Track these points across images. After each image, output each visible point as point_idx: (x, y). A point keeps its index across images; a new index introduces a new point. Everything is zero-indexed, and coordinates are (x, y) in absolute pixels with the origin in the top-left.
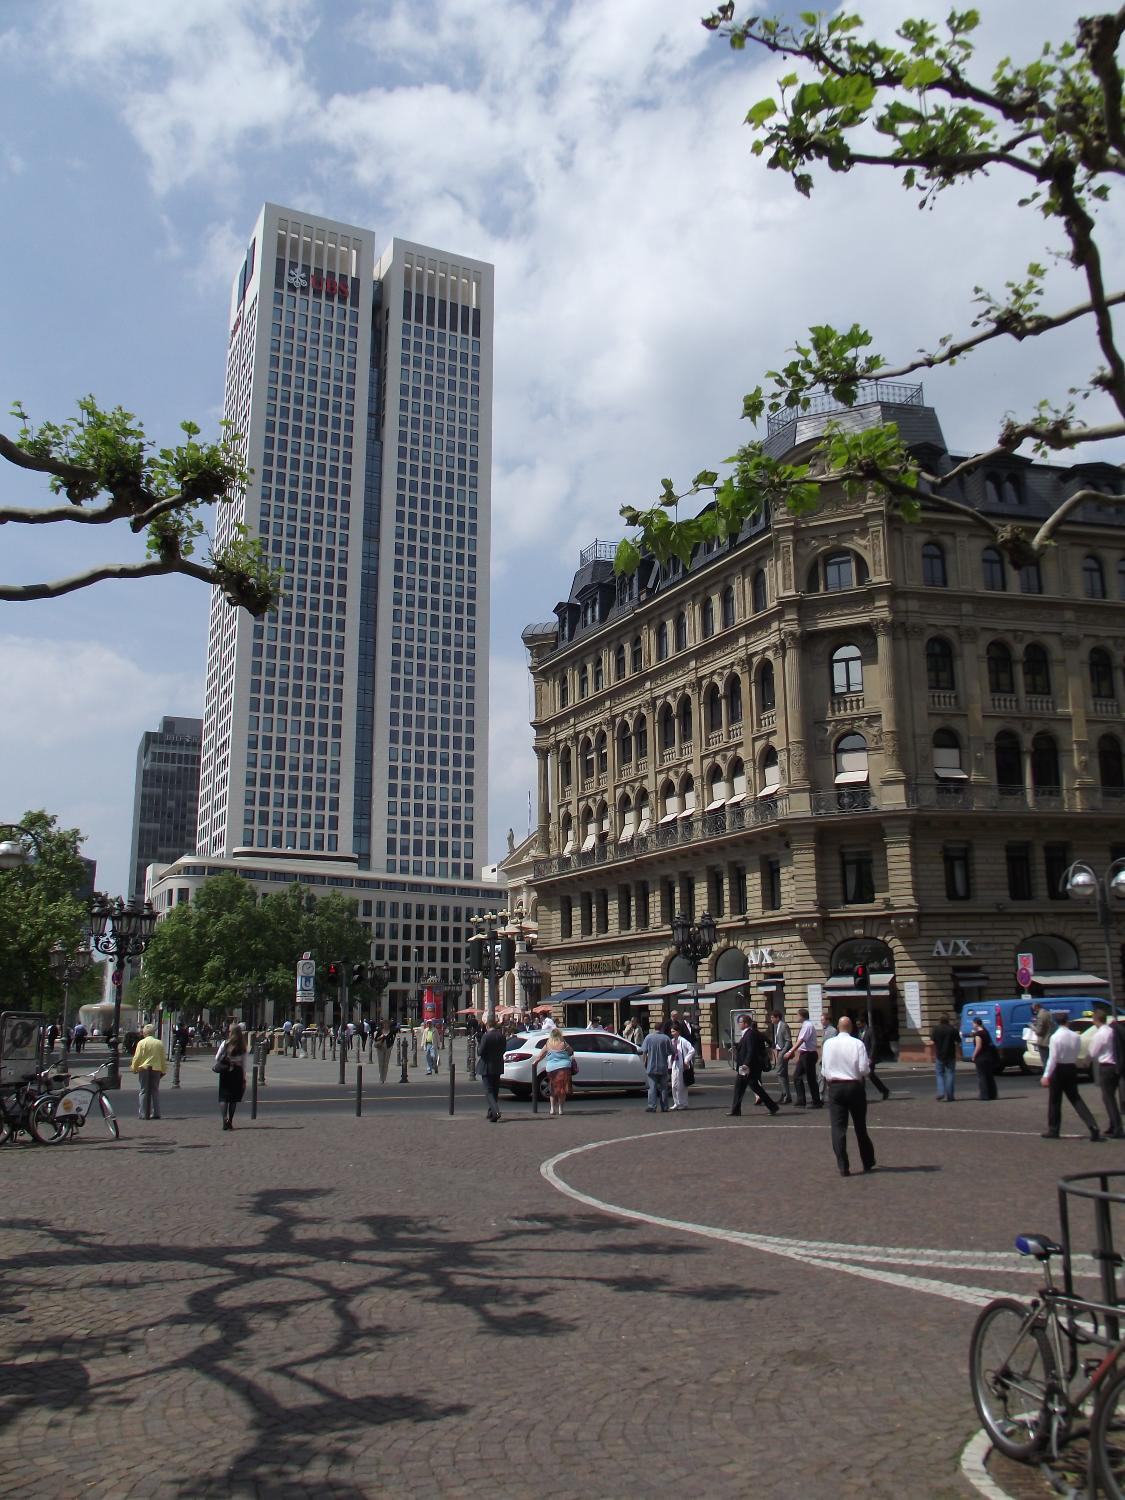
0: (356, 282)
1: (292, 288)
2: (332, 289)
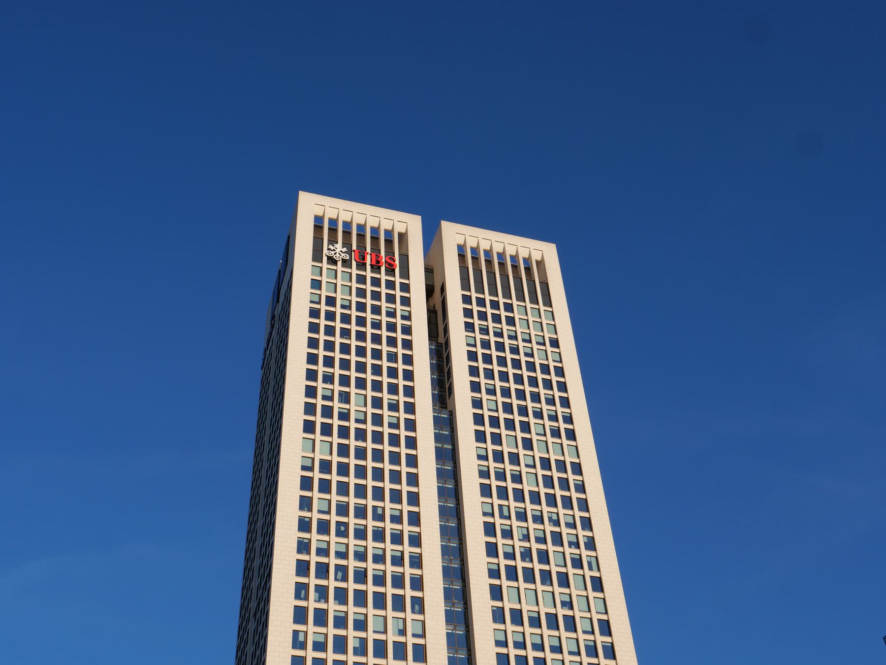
1: (332, 261)
2: (378, 262)
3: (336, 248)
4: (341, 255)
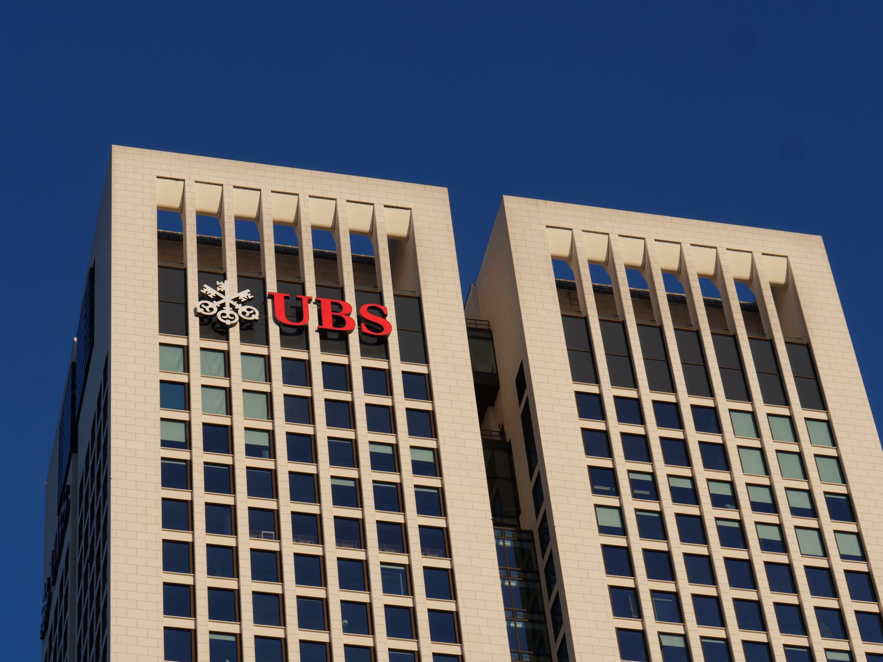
2: (340, 321)
3: (223, 293)
4: (236, 311)
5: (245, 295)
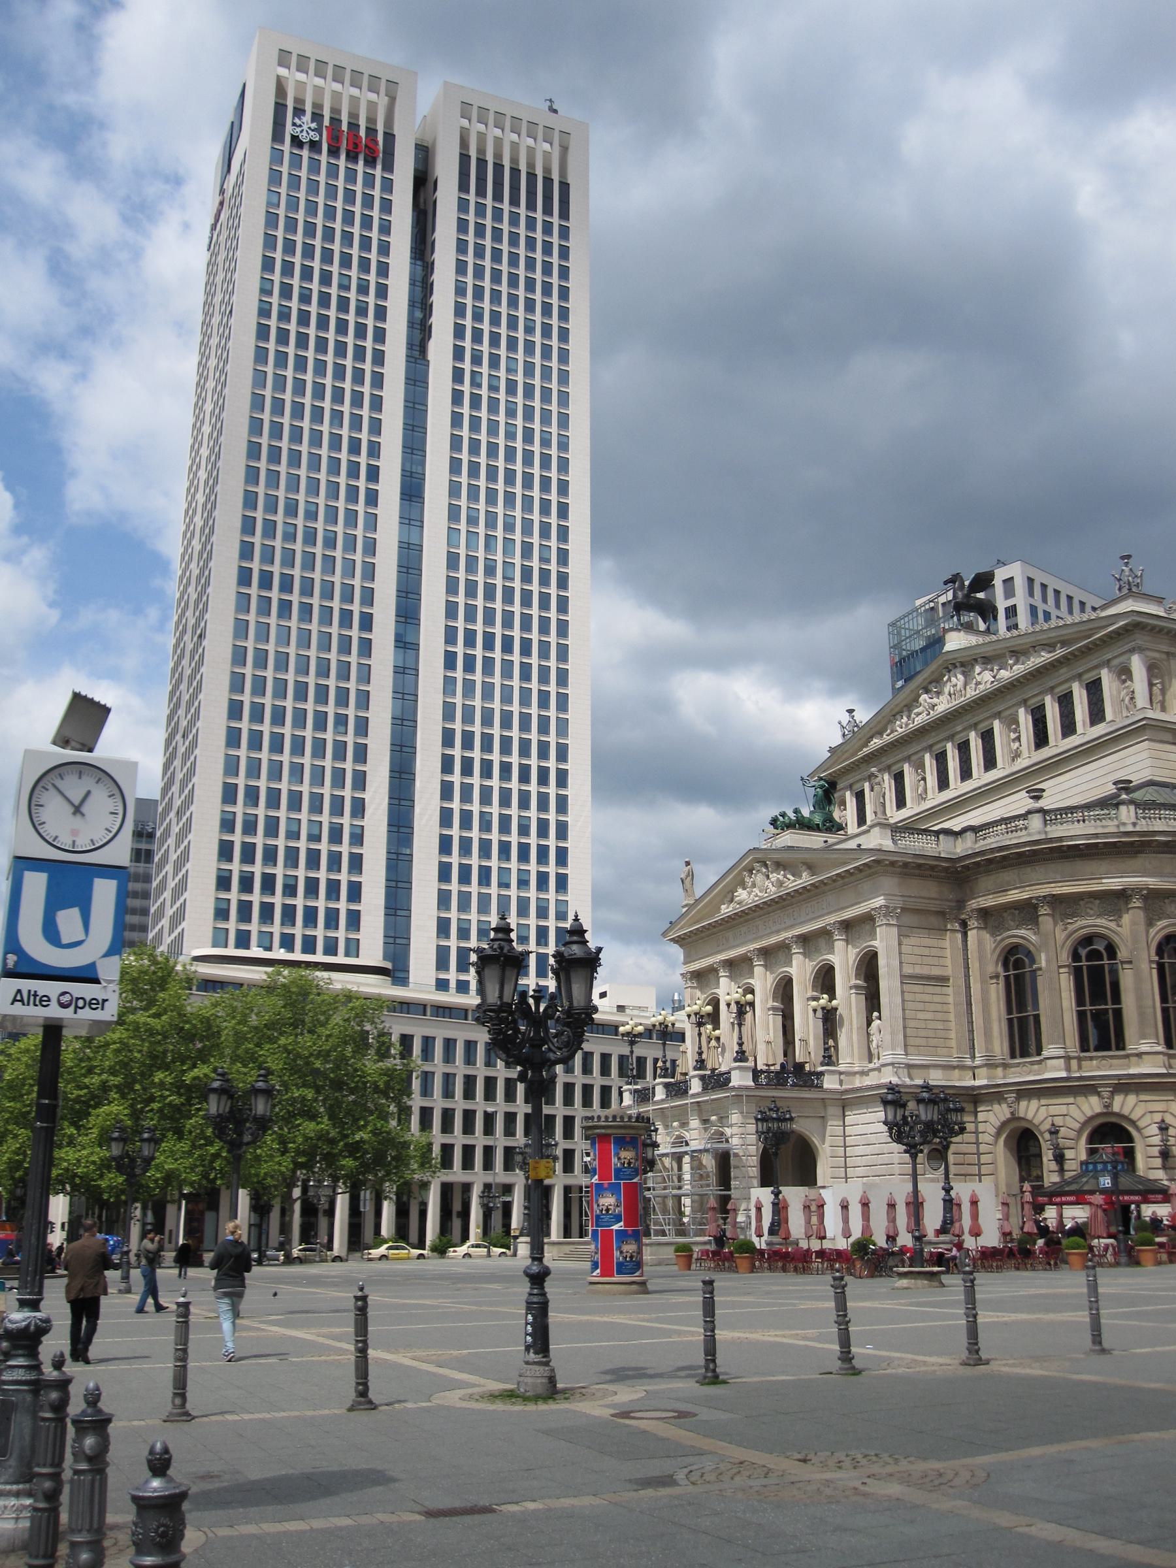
0: (390, 137)
1: (296, 142)
5: (314, 125)
